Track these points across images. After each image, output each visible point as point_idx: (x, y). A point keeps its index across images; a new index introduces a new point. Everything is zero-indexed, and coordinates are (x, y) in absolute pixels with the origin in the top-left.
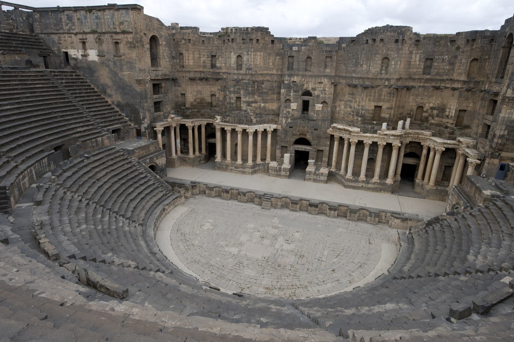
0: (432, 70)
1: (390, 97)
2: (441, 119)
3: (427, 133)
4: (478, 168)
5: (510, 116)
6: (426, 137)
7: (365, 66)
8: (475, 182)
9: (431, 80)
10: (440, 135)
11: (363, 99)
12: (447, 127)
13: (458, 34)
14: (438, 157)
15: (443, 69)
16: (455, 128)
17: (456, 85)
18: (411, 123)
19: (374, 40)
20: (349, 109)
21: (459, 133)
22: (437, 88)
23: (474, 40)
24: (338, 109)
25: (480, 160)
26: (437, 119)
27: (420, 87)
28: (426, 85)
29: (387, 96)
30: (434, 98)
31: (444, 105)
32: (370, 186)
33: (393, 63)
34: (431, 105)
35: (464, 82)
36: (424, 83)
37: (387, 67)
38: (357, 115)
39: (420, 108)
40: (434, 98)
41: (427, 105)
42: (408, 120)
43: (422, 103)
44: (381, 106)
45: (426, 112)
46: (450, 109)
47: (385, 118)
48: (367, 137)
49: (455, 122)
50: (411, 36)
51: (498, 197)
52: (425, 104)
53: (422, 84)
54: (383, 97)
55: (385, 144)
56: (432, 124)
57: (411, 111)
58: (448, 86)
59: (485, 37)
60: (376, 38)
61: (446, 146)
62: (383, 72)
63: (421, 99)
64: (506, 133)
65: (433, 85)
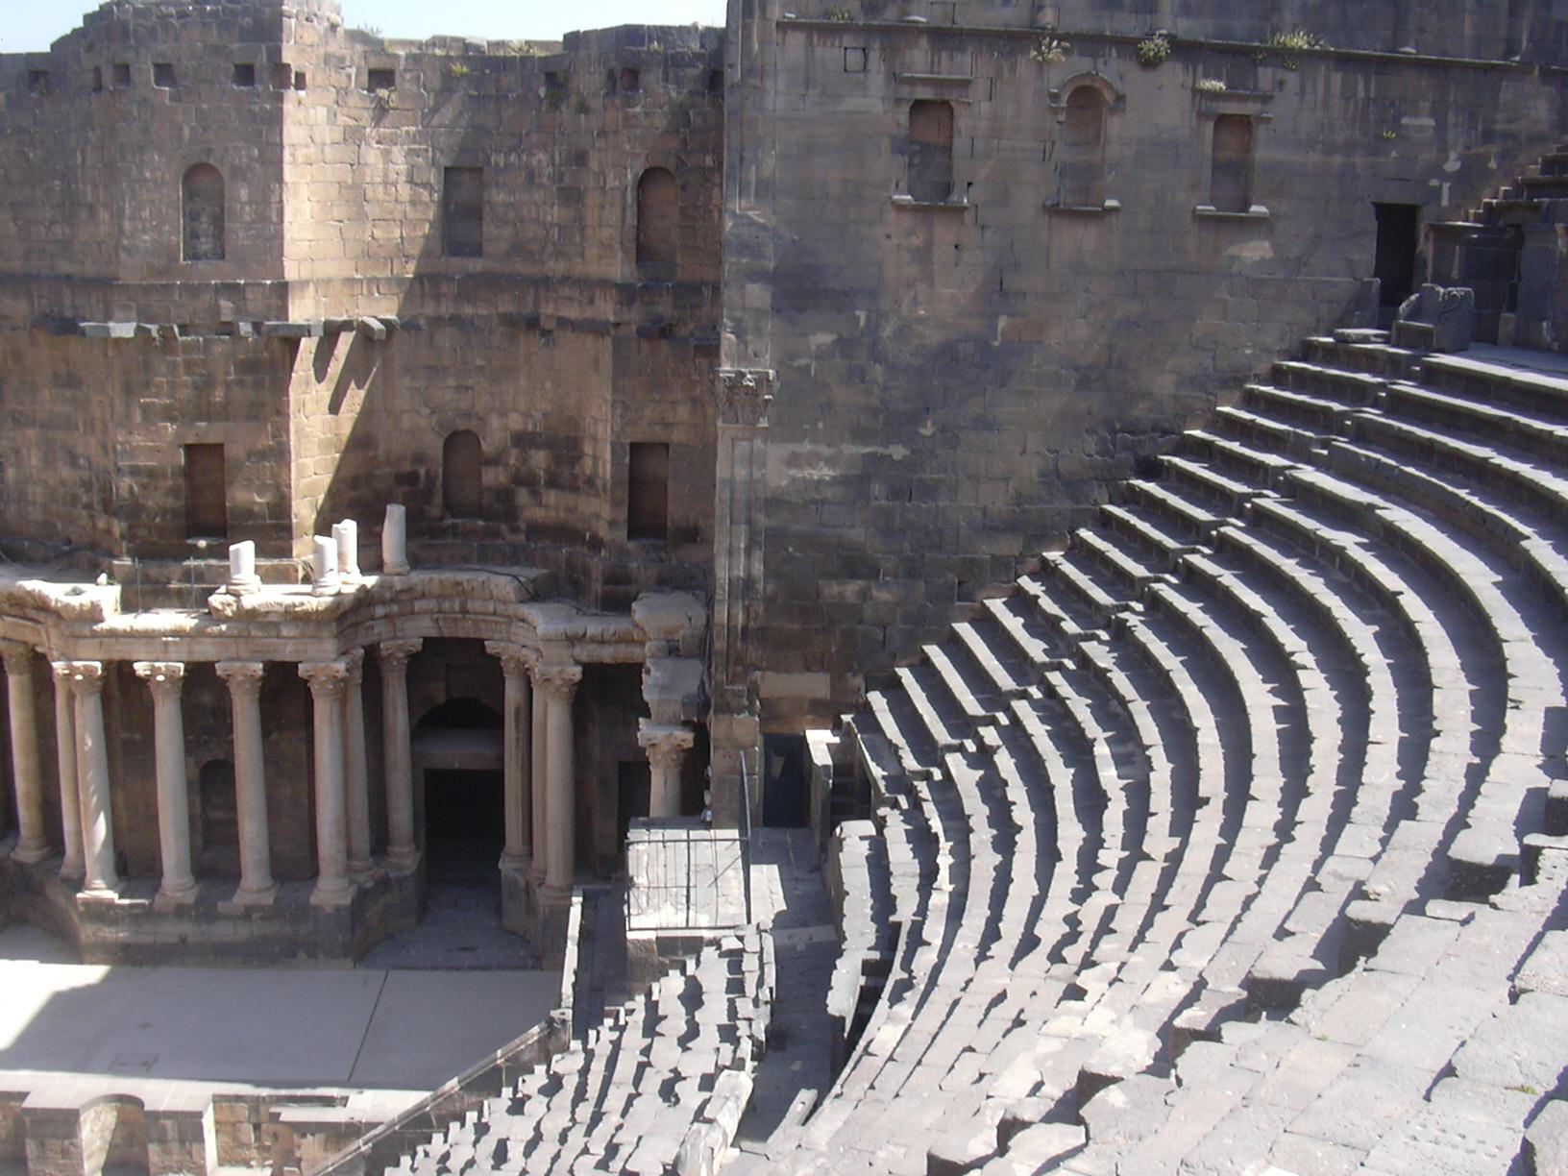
0: (489, 229)
1: (258, 385)
2: (568, 499)
3: (503, 584)
5: (757, 474)
6: (501, 608)
7: (104, 215)
9: (492, 283)
10: (557, 587)
11: (112, 406)
12: (596, 544)
13: (573, 40)
15: (537, 221)
16: (631, 545)
18: (416, 528)
19: (124, 72)
20: (66, 472)
21: (653, 572)
22: (532, 323)
24: (11, 473)
25: (686, 724)
26: (551, 497)
27: (437, 321)
28: (468, 310)
29: (240, 383)
30: (523, 381)
32: (223, 932)
33: (244, 194)
34: (515, 422)
35: (627, 294)
36: (460, 298)
37: (219, 222)
38: (109, 508)
39: (459, 441)
40: (523, 381)
41: (495, 422)
42: (395, 517)
43: (467, 415)
44: (220, 446)
45: (494, 461)
46: (595, 439)
47: (250, 513)
48: (149, 636)
49: (623, 514)
50: (336, 46)
52: (482, 420)
53: (446, 309)
54: (218, 395)
55: (258, 668)
56: (536, 530)
57: (419, 458)
58: (571, 312)
59: (672, 62)
60: (129, 56)
61: (585, 653)
62: (205, 245)
63: (458, 388)
64: (758, 568)
65: (502, 309)
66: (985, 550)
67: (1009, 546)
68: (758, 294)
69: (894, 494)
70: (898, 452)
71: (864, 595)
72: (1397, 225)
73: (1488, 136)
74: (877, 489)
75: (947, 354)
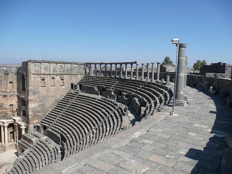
2: (2, 110)
4: (26, 130)
8: (27, 137)
12: (6, 114)
14: (6, 129)
17: (5, 94)
23: (8, 74)
31: (2, 103)
46: (5, 105)
51: (37, 140)
59: (12, 73)
61: (9, 123)
64: (32, 113)
66: (48, 109)
67: (50, 109)
68: (31, 93)
69: (42, 106)
70: (42, 103)
71: (40, 114)
72: (72, 84)
73: (77, 79)
74: (40, 106)
75: (45, 96)
